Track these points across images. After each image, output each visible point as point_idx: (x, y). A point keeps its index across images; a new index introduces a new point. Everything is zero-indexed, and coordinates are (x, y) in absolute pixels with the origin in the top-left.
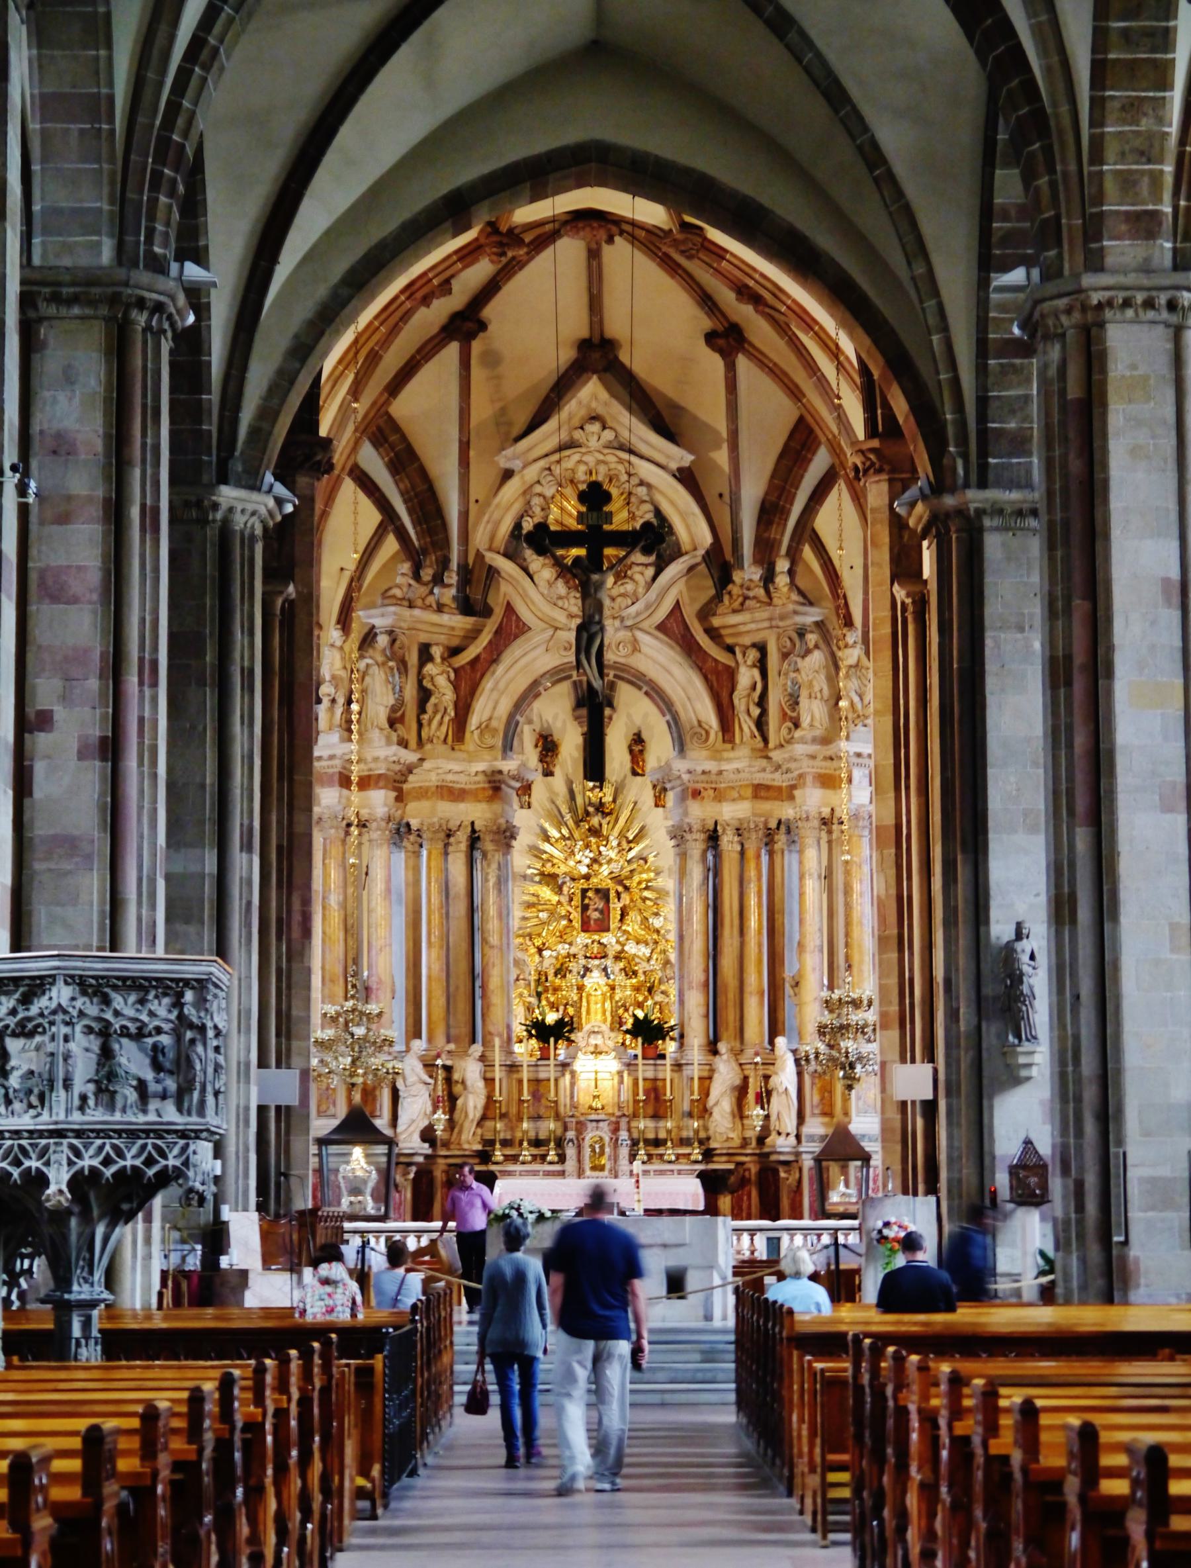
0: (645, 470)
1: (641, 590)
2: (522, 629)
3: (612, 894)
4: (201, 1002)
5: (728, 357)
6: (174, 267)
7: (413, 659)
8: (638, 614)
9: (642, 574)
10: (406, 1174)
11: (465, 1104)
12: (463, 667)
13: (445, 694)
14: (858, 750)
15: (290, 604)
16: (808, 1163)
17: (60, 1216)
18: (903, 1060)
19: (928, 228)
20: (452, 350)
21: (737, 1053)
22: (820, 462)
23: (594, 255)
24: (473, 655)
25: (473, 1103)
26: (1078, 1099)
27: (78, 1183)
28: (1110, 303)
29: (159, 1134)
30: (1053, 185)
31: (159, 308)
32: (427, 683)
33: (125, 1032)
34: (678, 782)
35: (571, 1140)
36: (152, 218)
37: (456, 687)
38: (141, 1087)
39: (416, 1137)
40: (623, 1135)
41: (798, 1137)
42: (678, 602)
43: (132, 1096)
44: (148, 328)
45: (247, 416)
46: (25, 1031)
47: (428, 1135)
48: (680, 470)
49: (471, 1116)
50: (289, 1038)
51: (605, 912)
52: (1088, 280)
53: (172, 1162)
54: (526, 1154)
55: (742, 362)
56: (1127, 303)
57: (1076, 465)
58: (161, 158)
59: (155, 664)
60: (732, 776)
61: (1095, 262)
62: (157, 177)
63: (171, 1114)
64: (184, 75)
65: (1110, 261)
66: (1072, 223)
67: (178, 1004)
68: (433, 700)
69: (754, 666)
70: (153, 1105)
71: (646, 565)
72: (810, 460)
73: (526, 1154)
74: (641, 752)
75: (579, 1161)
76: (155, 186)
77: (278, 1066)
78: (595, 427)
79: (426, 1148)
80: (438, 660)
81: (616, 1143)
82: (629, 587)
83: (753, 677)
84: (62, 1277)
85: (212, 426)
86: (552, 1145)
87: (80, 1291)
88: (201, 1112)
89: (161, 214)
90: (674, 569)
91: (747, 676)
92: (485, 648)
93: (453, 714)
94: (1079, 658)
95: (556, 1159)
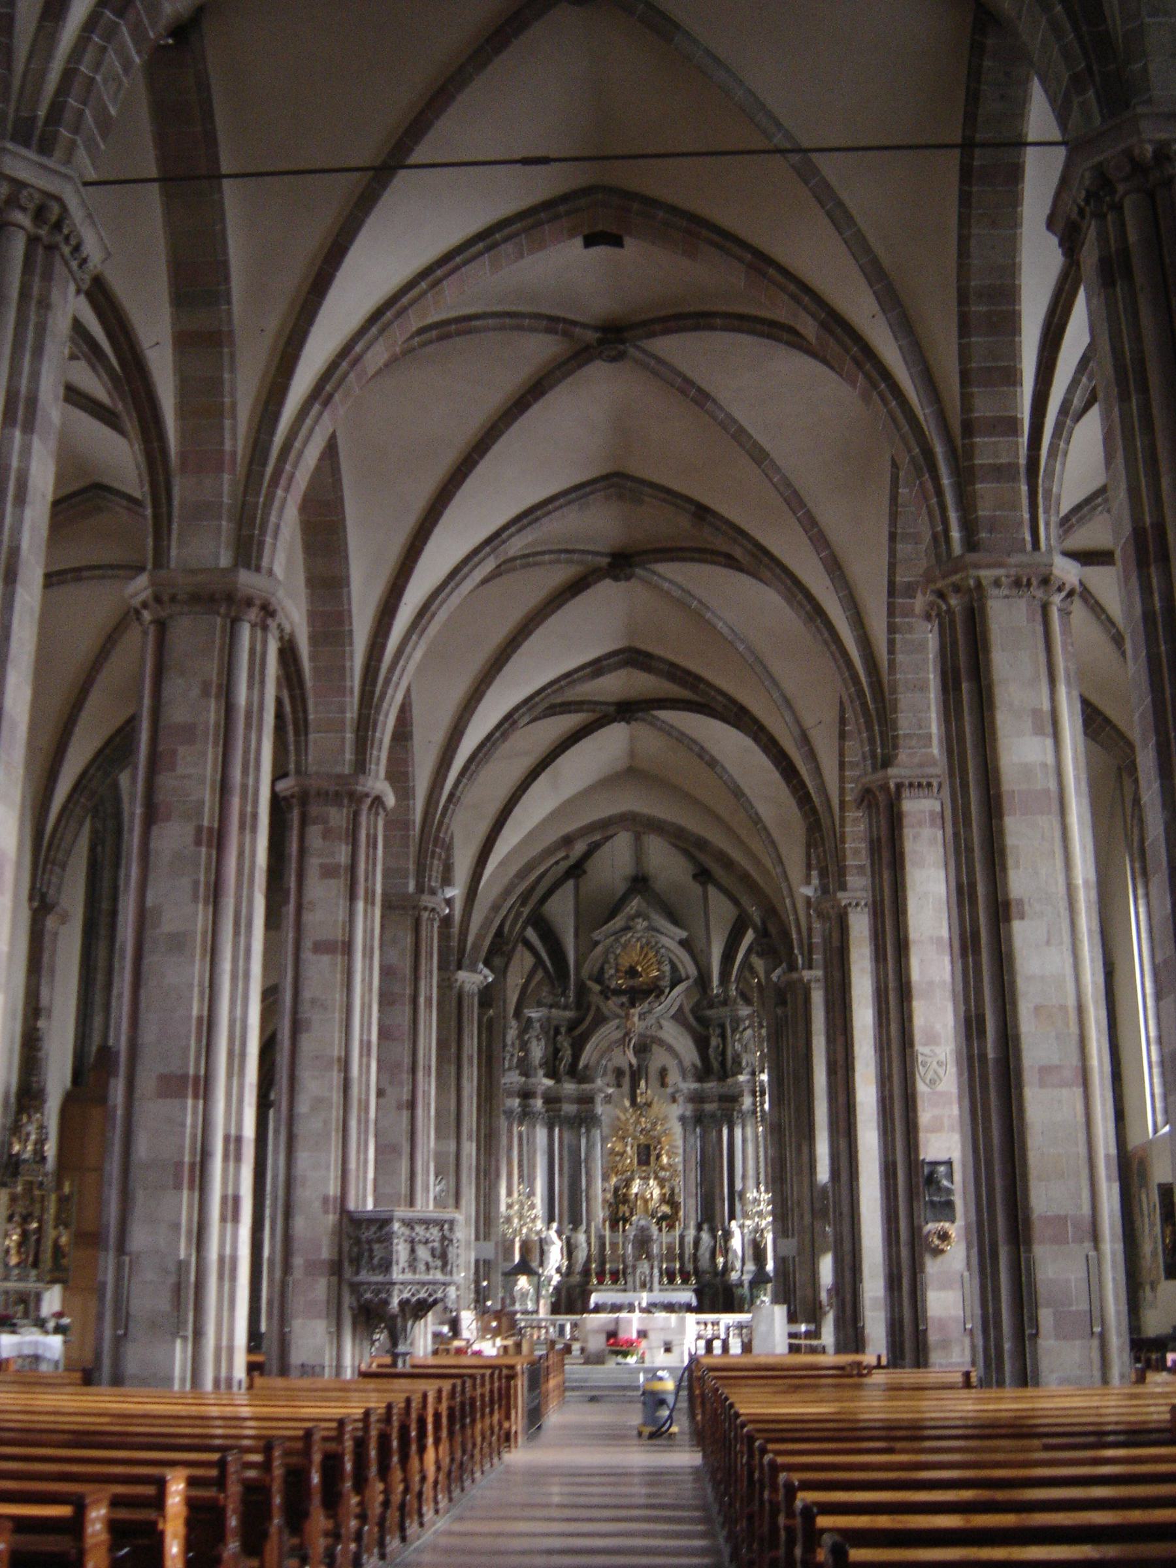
0: (665, 940)
4: (451, 1229)
5: (704, 884)
6: (440, 891)
7: (552, 1032)
13: (567, 1054)
15: (491, 1020)
16: (746, 1285)
17: (394, 1318)
19: (783, 851)
20: (570, 884)
21: (713, 1231)
22: (749, 936)
23: (638, 838)
25: (581, 1255)
26: (843, 1261)
27: (404, 1304)
28: (850, 904)
29: (434, 1283)
30: (824, 851)
31: (433, 910)
32: (559, 1046)
33: (420, 1242)
36: (431, 870)
37: (573, 1046)
38: (427, 1264)
43: (422, 1267)
44: (428, 919)
45: (471, 939)
46: (380, 1241)
47: (558, 1270)
51: (648, 1155)
52: (840, 895)
53: (439, 1295)
55: (712, 890)
56: (857, 905)
57: (837, 975)
58: (435, 845)
59: (430, 1067)
61: (843, 887)
62: (433, 852)
63: (439, 1276)
64: (446, 808)
65: (849, 885)
66: (832, 868)
67: (442, 1229)
70: (432, 1272)
73: (608, 1280)
76: (433, 857)
78: (640, 920)
81: (651, 1275)
84: (395, 1344)
85: (454, 943)
87: (401, 1348)
88: (451, 1273)
89: (434, 869)
91: (714, 1041)
94: (841, 1062)
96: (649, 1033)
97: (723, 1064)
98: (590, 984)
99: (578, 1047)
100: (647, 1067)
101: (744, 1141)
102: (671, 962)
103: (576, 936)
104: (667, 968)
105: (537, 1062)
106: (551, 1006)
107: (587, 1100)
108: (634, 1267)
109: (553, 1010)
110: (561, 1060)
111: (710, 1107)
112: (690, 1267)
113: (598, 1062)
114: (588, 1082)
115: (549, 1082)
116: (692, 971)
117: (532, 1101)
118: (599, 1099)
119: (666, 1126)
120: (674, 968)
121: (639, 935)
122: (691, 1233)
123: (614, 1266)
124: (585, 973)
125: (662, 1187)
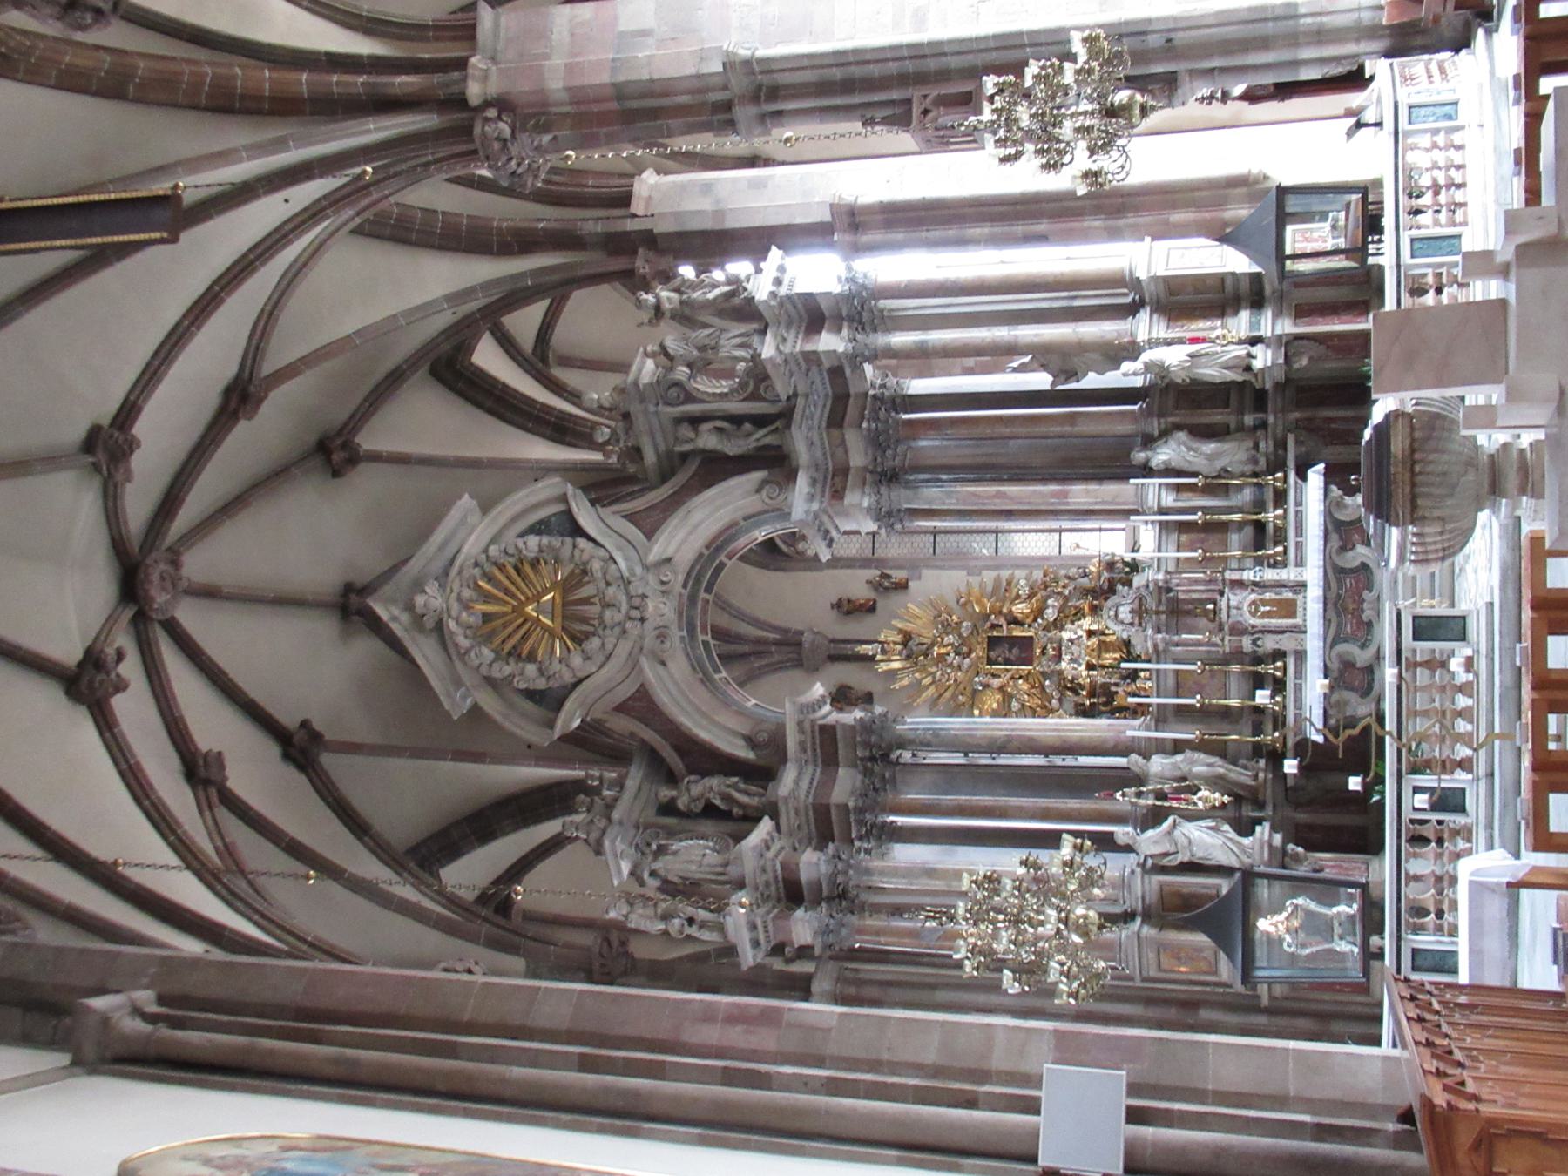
0: (472, 547)
1: (602, 553)
3: (995, 634)
8: (626, 559)
10: (1297, 858)
13: (713, 787)
14: (770, 280)
16: (1287, 327)
20: (327, 760)
24: (674, 754)
25: (1201, 765)
34: (825, 519)
35: (1254, 642)
37: (704, 774)
39: (1246, 841)
40: (1248, 575)
41: (1254, 341)
47: (1244, 828)
49: (1221, 770)
50: (983, 1076)
51: (1013, 641)
60: (819, 454)
68: (717, 802)
69: (696, 430)
71: (575, 546)
72: (504, 385)
74: (849, 601)
75: (1283, 632)
77: (1032, 1106)
78: (420, 600)
79: (1262, 831)
80: (674, 793)
81: (1258, 585)
82: (596, 566)
83: (710, 431)
86: (1259, 669)
90: (586, 516)
91: (708, 440)
93: (735, 779)
95: (1279, 664)
96: (678, 588)
97: (760, 421)
98: (558, 731)
99: (706, 760)
100: (833, 641)
102: (522, 535)
103: (478, 757)
104: (533, 541)
105: (713, 858)
106: (609, 820)
107: (826, 743)
108: (1238, 630)
109: (616, 815)
110: (727, 798)
111: (858, 457)
114: (784, 736)
115: (766, 825)
117: (805, 875)
118: (835, 717)
119: (953, 604)
120: (538, 529)
121: (455, 607)
123: (1234, 685)
124: (541, 738)
125: (1079, 614)
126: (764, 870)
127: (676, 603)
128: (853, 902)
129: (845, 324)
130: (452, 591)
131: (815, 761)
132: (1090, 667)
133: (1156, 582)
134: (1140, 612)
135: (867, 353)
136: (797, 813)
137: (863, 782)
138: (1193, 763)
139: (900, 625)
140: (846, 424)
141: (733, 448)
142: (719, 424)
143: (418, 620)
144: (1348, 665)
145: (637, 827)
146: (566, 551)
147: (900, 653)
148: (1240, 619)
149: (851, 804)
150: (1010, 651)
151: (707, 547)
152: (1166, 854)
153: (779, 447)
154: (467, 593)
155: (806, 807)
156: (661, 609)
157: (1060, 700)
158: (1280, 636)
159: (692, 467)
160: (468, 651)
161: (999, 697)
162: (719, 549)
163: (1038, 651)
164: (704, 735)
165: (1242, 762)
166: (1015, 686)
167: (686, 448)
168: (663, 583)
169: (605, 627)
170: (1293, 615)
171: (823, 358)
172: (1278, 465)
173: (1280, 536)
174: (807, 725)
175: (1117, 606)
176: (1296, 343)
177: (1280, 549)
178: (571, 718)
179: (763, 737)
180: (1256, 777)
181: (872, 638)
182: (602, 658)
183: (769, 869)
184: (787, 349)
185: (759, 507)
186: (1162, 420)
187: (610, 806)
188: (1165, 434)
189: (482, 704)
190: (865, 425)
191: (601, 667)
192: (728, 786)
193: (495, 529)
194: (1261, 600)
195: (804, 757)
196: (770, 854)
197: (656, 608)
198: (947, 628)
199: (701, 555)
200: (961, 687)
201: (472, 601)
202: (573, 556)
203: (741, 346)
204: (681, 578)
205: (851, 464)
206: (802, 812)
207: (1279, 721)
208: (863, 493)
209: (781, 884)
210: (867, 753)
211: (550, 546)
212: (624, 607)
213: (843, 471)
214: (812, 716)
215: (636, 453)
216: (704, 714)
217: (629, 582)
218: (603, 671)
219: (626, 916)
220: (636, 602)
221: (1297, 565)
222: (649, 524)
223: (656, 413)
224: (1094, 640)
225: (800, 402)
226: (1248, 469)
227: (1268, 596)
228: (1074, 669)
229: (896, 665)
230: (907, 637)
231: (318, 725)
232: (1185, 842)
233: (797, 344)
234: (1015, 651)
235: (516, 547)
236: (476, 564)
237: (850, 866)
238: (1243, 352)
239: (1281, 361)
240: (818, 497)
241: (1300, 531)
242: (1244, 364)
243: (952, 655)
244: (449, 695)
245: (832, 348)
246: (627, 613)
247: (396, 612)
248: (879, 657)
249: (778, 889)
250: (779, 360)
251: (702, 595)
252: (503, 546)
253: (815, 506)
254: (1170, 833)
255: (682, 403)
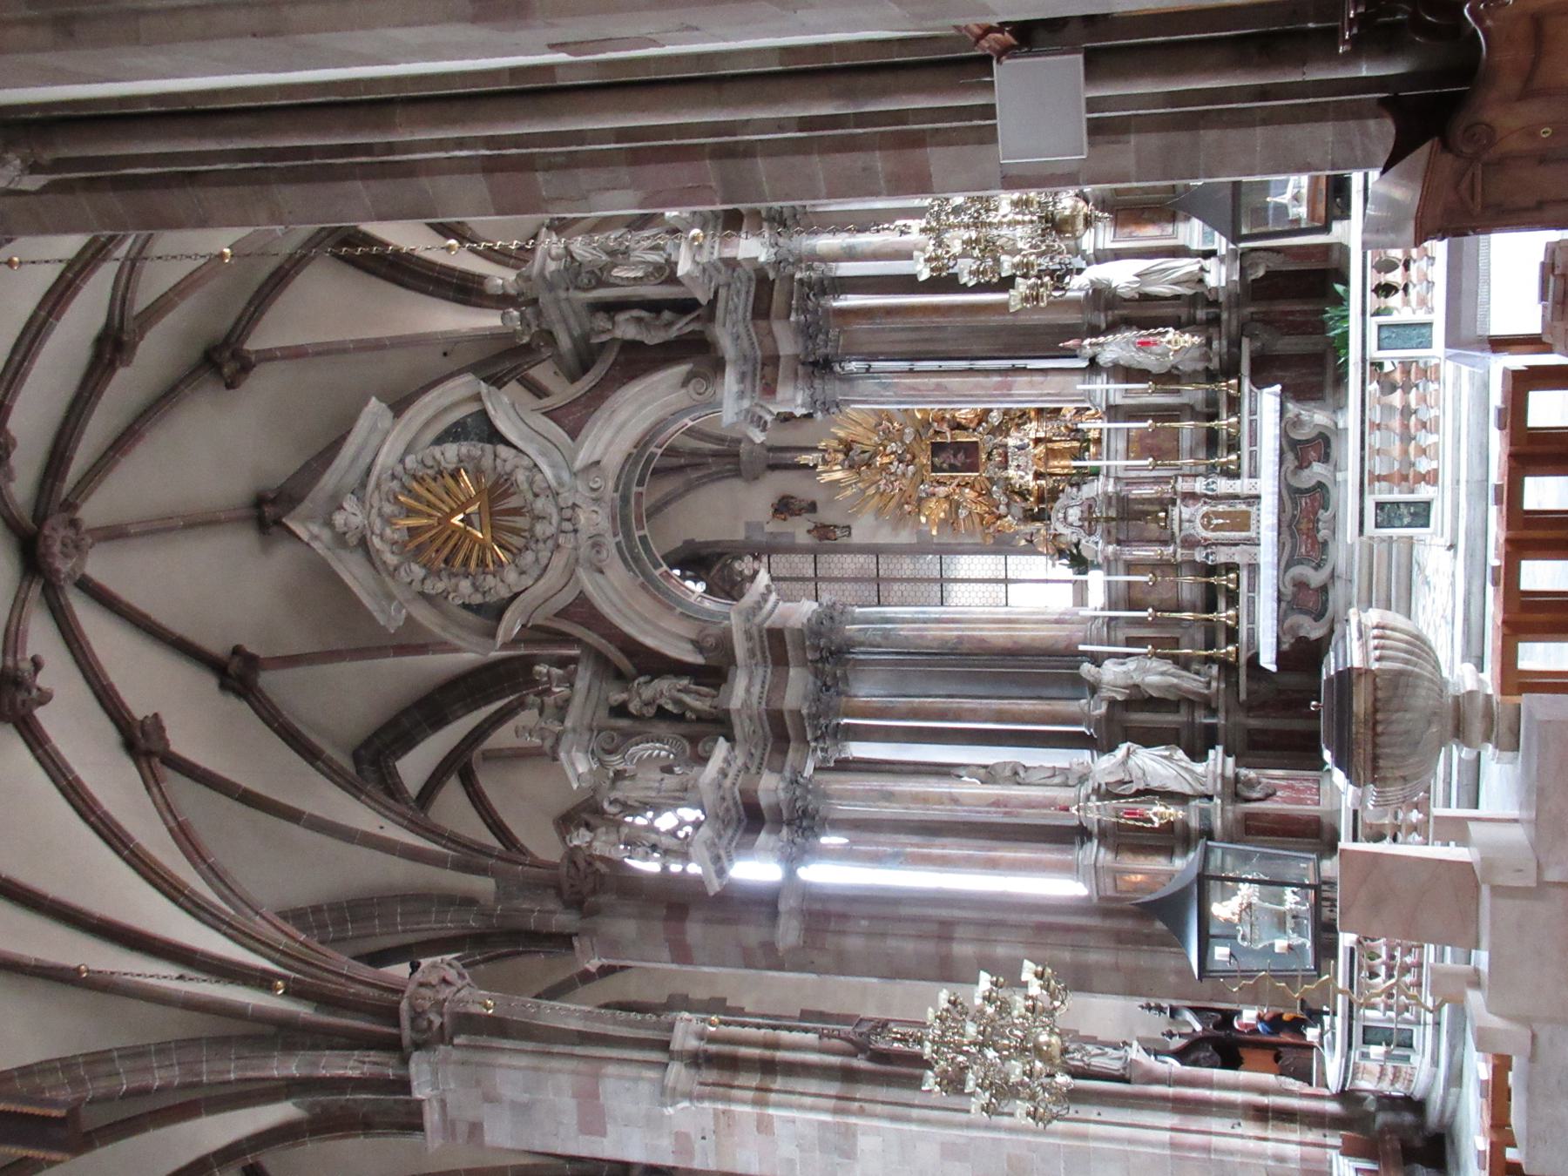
0: (387, 457)
1: (526, 462)
2: (582, 600)
3: (939, 440)
7: (623, 723)
8: (553, 466)
9: (505, 461)
10: (1250, 784)
11: (1158, 687)
12: (635, 666)
18: (988, 136)
39: (1199, 768)
40: (1199, 486)
41: (1209, 254)
42: (544, 414)
48: (390, 414)
49: (1175, 681)
51: (958, 447)
54: (1224, 615)
60: (745, 344)
68: (670, 707)
73: (1224, 615)
75: (1236, 545)
78: (339, 519)
79: (1215, 754)
80: (625, 696)
82: (521, 476)
86: (1212, 580)
91: (626, 328)
92: (610, 642)
95: (1232, 576)
99: (656, 665)
101: (851, 255)
102: (439, 441)
104: (451, 451)
108: (1190, 543)
110: (678, 702)
111: (788, 346)
112: (1192, 394)
113: (690, 614)
115: (722, 747)
116: (464, 385)
117: (764, 801)
120: (454, 433)
122: (1104, 389)
126: (723, 799)
127: (608, 510)
128: (814, 818)
129: (765, 224)
130: (372, 506)
131: (765, 662)
132: (1038, 476)
133: (1105, 493)
134: (1089, 522)
135: (791, 260)
136: (751, 718)
137: (815, 683)
138: (1146, 671)
139: (841, 434)
140: (772, 315)
141: (653, 338)
142: (636, 313)
143: (340, 539)
144: (1301, 585)
145: (591, 730)
146: (487, 462)
147: (842, 464)
148: (1192, 532)
149: (804, 712)
150: (955, 456)
151: (635, 447)
152: (1122, 782)
153: (702, 332)
154: (388, 509)
155: (759, 714)
156: (594, 519)
157: (1008, 505)
158: (1233, 548)
159: (610, 357)
160: (396, 569)
161: (946, 506)
162: (646, 445)
163: (984, 457)
164: (649, 642)
165: (1195, 667)
166: (961, 494)
167: (605, 338)
168: (594, 490)
169: (537, 541)
170: (1246, 527)
171: (744, 263)
172: (1230, 369)
173: (1234, 446)
174: (756, 634)
175: (1067, 507)
176: (1253, 254)
177: (1233, 457)
178: (511, 624)
179: (711, 641)
180: (1208, 684)
181: (813, 445)
182: (535, 572)
183: (728, 796)
184: (704, 258)
185: (686, 403)
186: (1110, 313)
187: (562, 709)
188: (1112, 328)
189: (414, 615)
190: (793, 318)
191: (537, 580)
192: (679, 691)
193: (408, 437)
194: (1213, 512)
195: (753, 662)
196: (728, 783)
197: (588, 519)
198: (888, 436)
199: (630, 455)
200: (907, 495)
201: (395, 516)
202: (495, 468)
203: (655, 248)
204: (611, 484)
205: (781, 353)
206: (756, 718)
207: (1232, 635)
208: (796, 387)
209: (741, 808)
210: (818, 655)
211: (470, 457)
212: (555, 520)
213: (772, 360)
214: (758, 619)
215: (549, 337)
216: (646, 620)
217: (558, 494)
218: (541, 582)
219: (590, 844)
220: (568, 513)
221: (1251, 477)
222: (573, 419)
223: (567, 299)
224: (1041, 448)
225: (722, 292)
226: (1200, 366)
227: (1221, 508)
228: (1022, 477)
229: (838, 475)
230: (847, 447)
231: (251, 649)
232: (1140, 774)
233: (716, 250)
234: (961, 456)
235: (434, 458)
236: (394, 477)
237: (809, 791)
238: (1196, 268)
239: (1236, 277)
240: (748, 393)
241: (1254, 440)
242: (1196, 279)
243: (896, 463)
244: (383, 611)
245: (753, 255)
246: (559, 524)
247: (315, 529)
248: (820, 468)
249: (738, 812)
250: (697, 273)
251: (635, 489)
252: (419, 457)
253: (746, 404)
254: (1124, 762)
255: (594, 288)
